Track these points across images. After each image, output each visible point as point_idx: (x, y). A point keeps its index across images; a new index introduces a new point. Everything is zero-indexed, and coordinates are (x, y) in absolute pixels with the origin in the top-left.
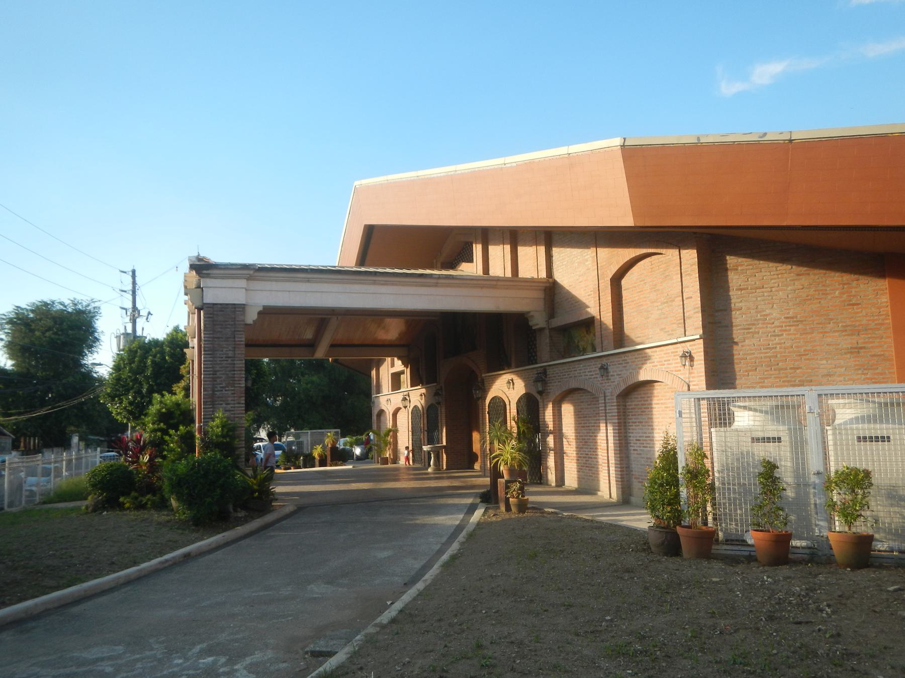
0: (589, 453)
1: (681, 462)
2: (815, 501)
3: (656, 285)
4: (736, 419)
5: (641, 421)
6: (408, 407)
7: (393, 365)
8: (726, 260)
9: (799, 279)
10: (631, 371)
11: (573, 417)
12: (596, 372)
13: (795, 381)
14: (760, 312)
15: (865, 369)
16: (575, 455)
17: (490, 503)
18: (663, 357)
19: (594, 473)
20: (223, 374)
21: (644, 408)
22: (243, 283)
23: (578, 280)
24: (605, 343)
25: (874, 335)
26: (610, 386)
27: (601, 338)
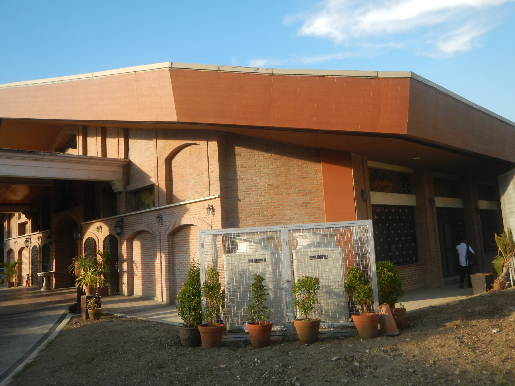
0: (150, 273)
1: (203, 279)
2: (286, 299)
3: (193, 164)
4: (239, 248)
5: (183, 250)
6: (29, 246)
7: (20, 218)
8: (235, 149)
11: (140, 249)
12: (155, 220)
13: (273, 223)
14: (254, 181)
15: (310, 216)
16: (141, 274)
17: (76, 313)
18: (197, 209)
19: (153, 286)
23: (145, 160)
24: (161, 201)
25: (314, 196)
26: (163, 228)
27: (159, 197)
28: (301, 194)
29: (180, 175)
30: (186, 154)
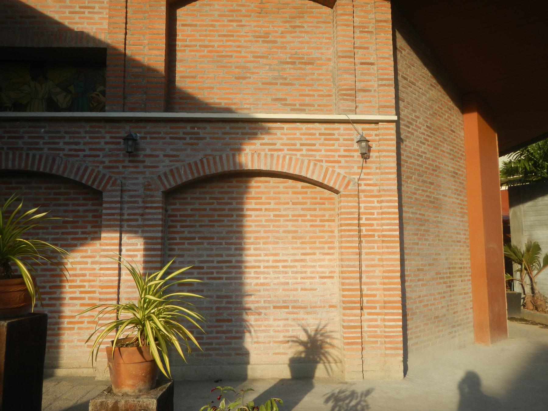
5: (209, 235)
9: (432, 90)
10: (209, 152)
21: (219, 216)
26: (143, 173)
28: (451, 157)
29: (210, 49)
30: (243, 6)
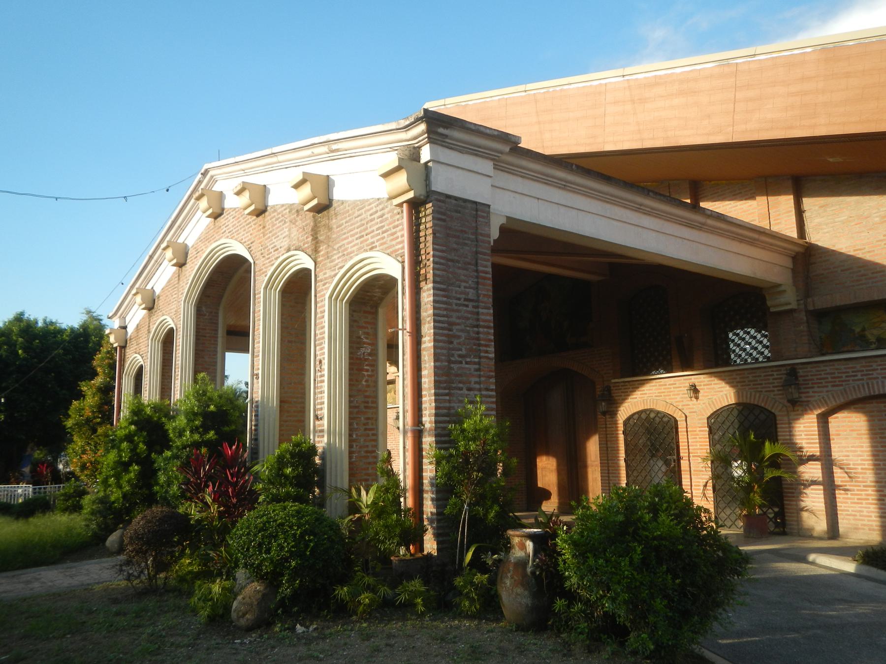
20: (462, 331)
22: (486, 166)
